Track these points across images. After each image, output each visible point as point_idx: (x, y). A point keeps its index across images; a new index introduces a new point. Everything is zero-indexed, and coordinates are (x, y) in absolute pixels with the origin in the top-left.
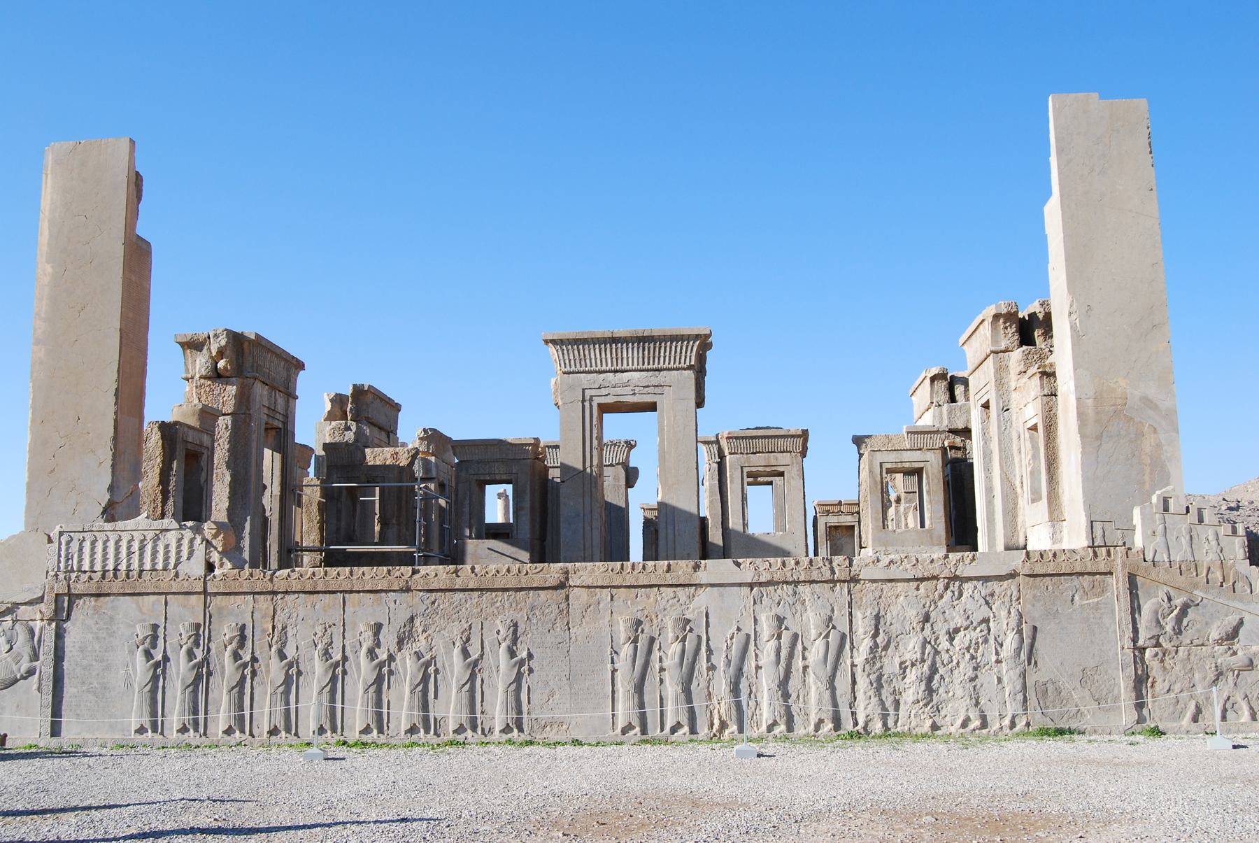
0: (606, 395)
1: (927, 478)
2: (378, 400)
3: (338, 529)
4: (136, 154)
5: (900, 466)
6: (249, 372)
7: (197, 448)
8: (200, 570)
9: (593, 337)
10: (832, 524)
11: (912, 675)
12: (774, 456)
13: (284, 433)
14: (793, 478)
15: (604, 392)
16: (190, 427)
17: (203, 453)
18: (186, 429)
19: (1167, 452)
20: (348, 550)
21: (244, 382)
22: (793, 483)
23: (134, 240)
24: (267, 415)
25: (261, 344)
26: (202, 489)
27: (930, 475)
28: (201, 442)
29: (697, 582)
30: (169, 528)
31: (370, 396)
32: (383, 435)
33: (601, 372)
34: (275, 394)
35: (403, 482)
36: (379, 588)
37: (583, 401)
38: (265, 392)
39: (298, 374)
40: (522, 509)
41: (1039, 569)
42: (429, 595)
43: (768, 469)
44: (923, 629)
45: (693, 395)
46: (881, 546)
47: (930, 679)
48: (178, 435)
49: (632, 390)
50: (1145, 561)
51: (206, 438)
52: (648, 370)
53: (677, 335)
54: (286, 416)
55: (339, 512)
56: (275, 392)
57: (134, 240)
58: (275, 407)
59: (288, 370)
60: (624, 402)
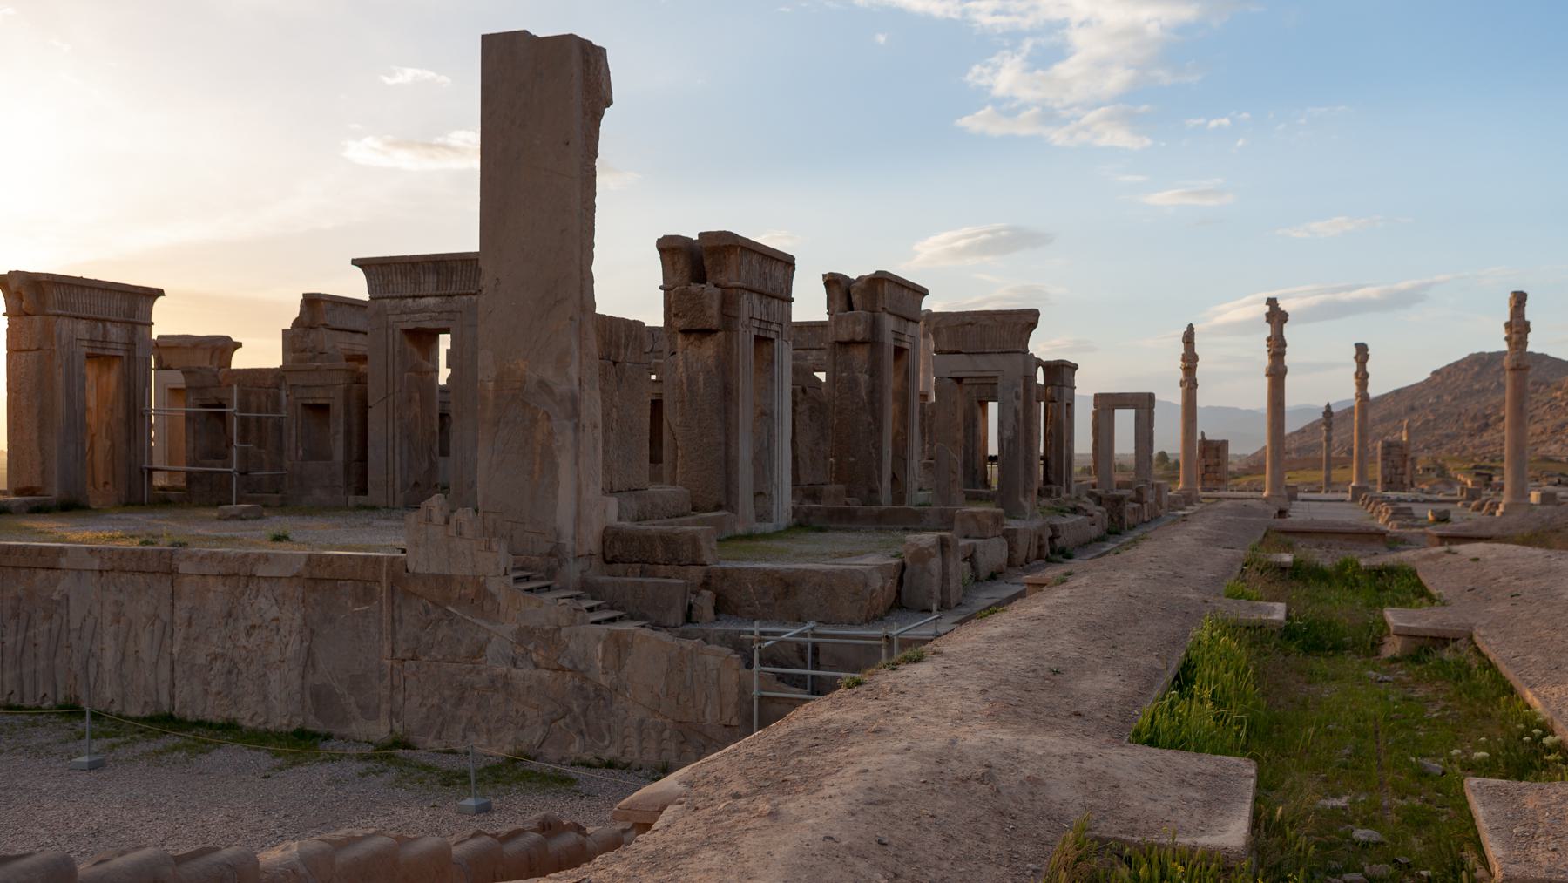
11: (217, 665)
15: (405, 317)
19: (558, 441)
33: (402, 298)
41: (317, 573)
44: (227, 624)
47: (230, 672)
50: (407, 571)
52: (440, 296)
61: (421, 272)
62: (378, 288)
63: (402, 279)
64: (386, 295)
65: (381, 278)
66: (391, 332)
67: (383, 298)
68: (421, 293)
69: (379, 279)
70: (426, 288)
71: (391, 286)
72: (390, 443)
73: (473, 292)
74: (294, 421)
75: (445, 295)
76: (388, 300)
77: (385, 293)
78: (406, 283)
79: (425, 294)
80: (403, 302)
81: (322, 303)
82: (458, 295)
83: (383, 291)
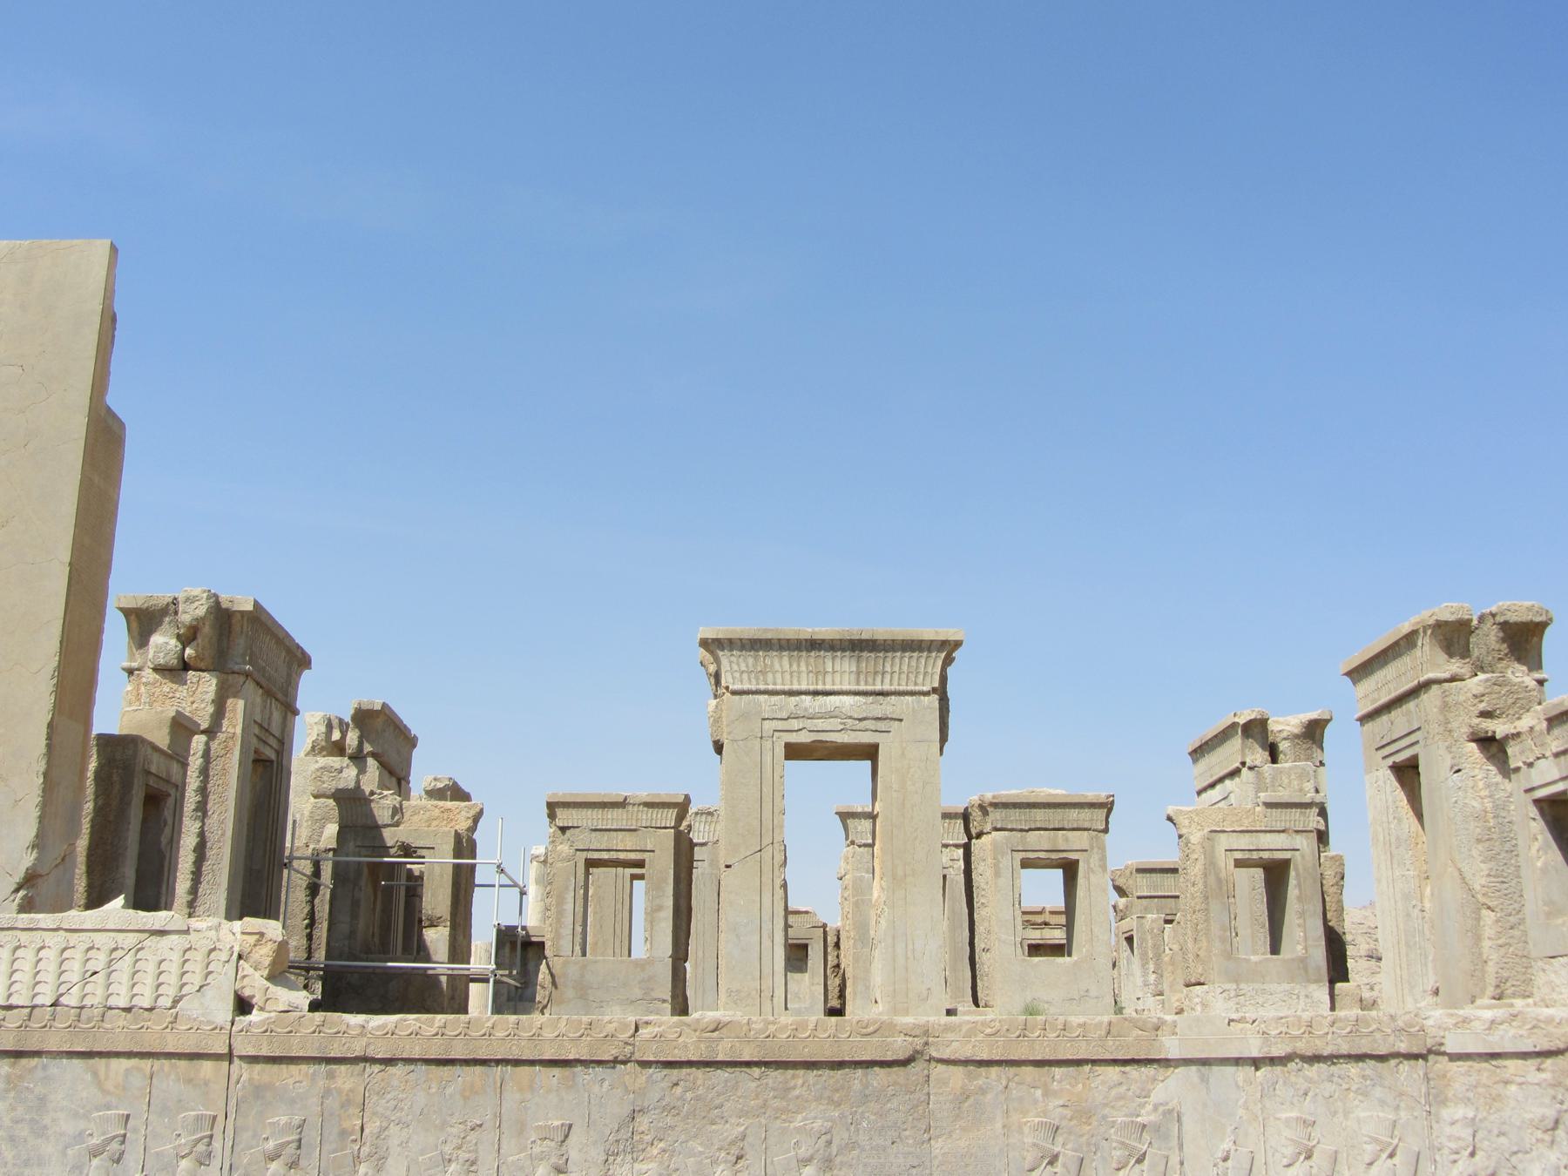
0: (801, 730)
1: (1298, 875)
2: (392, 728)
3: (352, 934)
4: (118, 270)
5: (1255, 855)
6: (237, 663)
7: (162, 786)
8: (223, 1011)
9: (782, 637)
10: (1033, 942)
12: (1063, 835)
13: (277, 767)
14: (1093, 871)
15: (795, 724)
16: (156, 748)
17: (169, 795)
18: (150, 751)
20: (430, 972)
21: (227, 680)
22: (1093, 878)
23: (103, 414)
24: (257, 737)
25: (259, 620)
26: (162, 857)
27: (1301, 871)
28: (168, 773)
29: (1162, 1056)
30: (167, 928)
31: (379, 722)
32: (394, 780)
34: (271, 703)
35: (369, 864)
36: (571, 1057)
37: (761, 738)
38: (258, 700)
39: (300, 675)
40: (660, 908)
42: (666, 1071)
43: (1054, 856)
46: (1230, 982)
48: (137, 761)
49: (841, 723)
51: (175, 767)
53: (913, 641)
54: (281, 742)
55: (355, 904)
56: (271, 700)
57: (103, 414)
58: (269, 724)
59: (289, 667)
60: (827, 742)
62: (745, 676)
63: (791, 665)
64: (762, 687)
65: (751, 661)
66: (770, 742)
68: (828, 687)
71: (770, 676)
72: (767, 926)
73: (925, 689)
74: (572, 887)
76: (766, 696)
77: (758, 684)
78: (799, 673)
79: (837, 687)
80: (793, 699)
83: (753, 681)
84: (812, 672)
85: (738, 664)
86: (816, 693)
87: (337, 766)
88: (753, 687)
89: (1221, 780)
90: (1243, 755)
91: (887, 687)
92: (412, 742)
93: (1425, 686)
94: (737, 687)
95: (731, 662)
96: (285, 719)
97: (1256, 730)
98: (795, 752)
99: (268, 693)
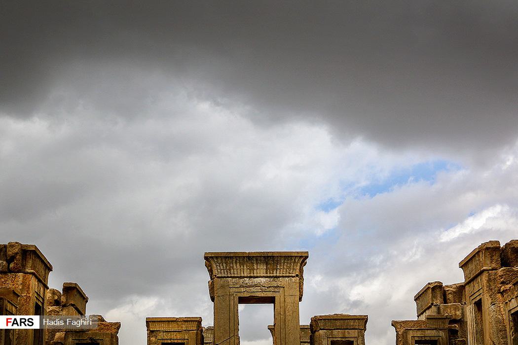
15: (243, 290)
45: (298, 293)
61: (255, 262)
62: (222, 271)
63: (240, 267)
64: (229, 275)
65: (224, 265)
66: (232, 297)
67: (226, 277)
68: (255, 275)
69: (223, 265)
70: (258, 272)
75: (272, 277)
78: (243, 269)
79: (258, 275)
80: (242, 280)
81: (75, 290)
82: (283, 277)
84: (249, 269)
85: (220, 266)
86: (251, 277)
87: (57, 310)
88: (226, 276)
89: (425, 311)
90: (433, 301)
91: (278, 275)
92: (85, 300)
93: (482, 272)
94: (220, 275)
95: (217, 266)
96: (44, 290)
97: (438, 290)
98: (243, 300)
99: (39, 281)
